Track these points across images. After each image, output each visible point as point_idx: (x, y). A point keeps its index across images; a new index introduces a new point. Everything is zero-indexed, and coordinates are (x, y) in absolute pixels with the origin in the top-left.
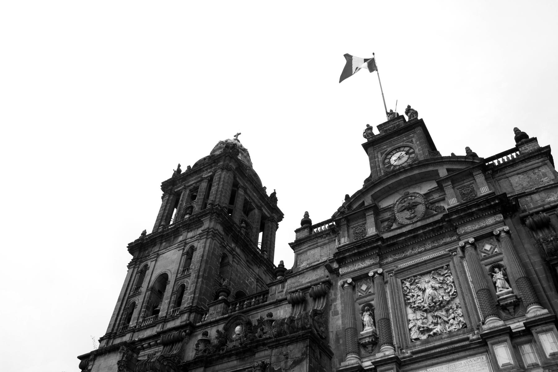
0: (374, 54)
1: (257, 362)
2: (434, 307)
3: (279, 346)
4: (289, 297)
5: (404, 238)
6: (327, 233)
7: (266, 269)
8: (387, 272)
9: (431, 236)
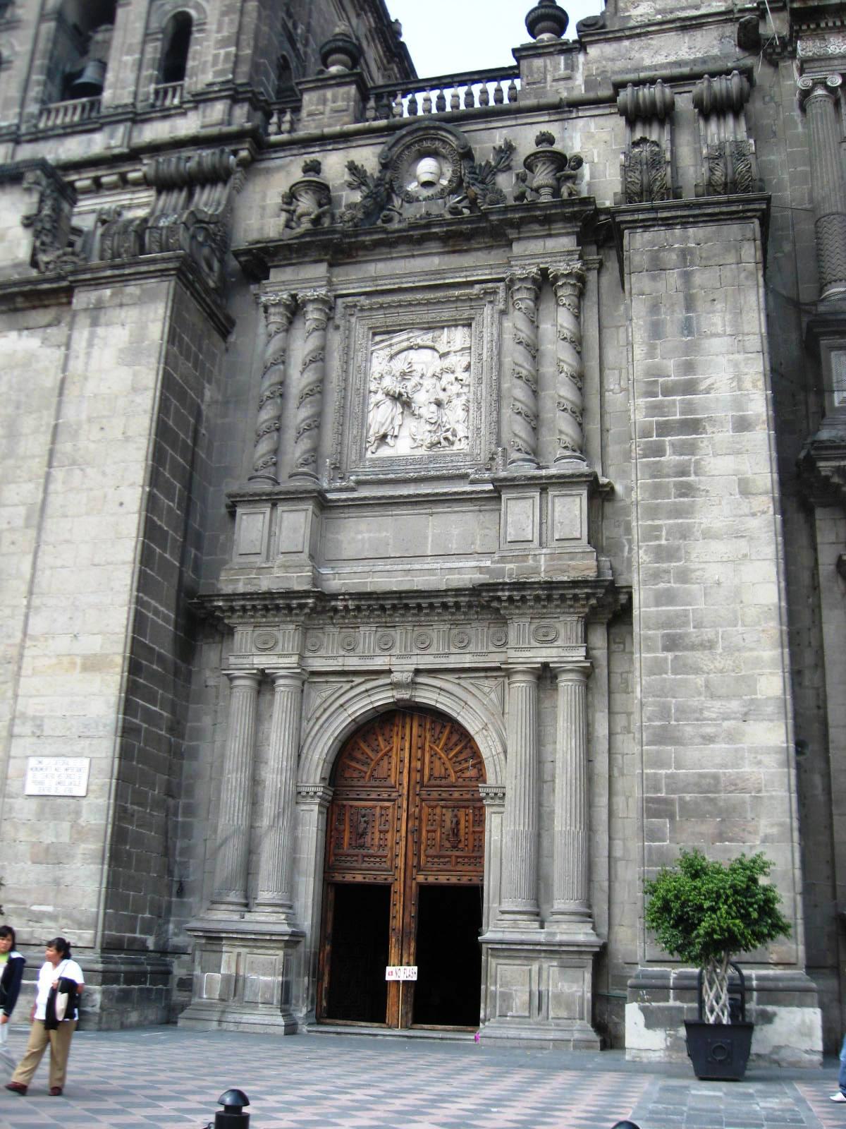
1: (277, 295)
3: (654, 226)
4: (625, 96)
7: (373, 25)
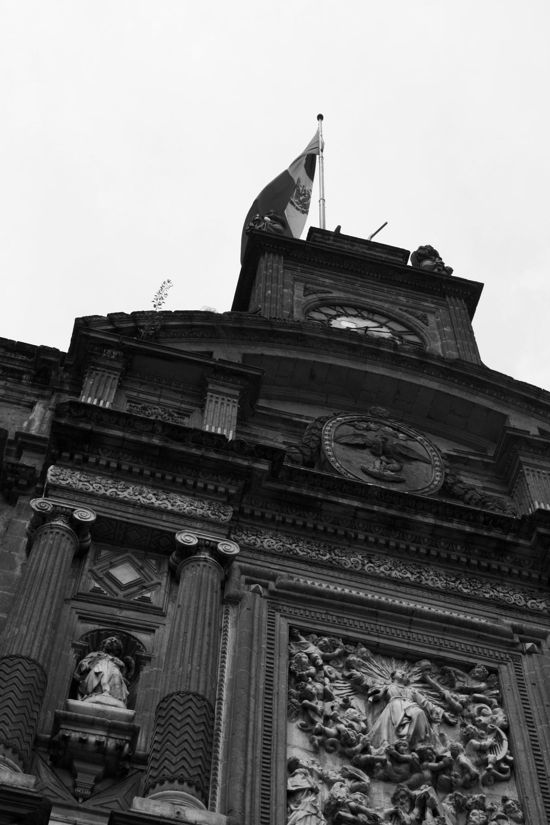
0: (320, 117)
2: (414, 767)
5: (356, 504)
6: (13, 370)
8: (244, 572)
9: (454, 557)
